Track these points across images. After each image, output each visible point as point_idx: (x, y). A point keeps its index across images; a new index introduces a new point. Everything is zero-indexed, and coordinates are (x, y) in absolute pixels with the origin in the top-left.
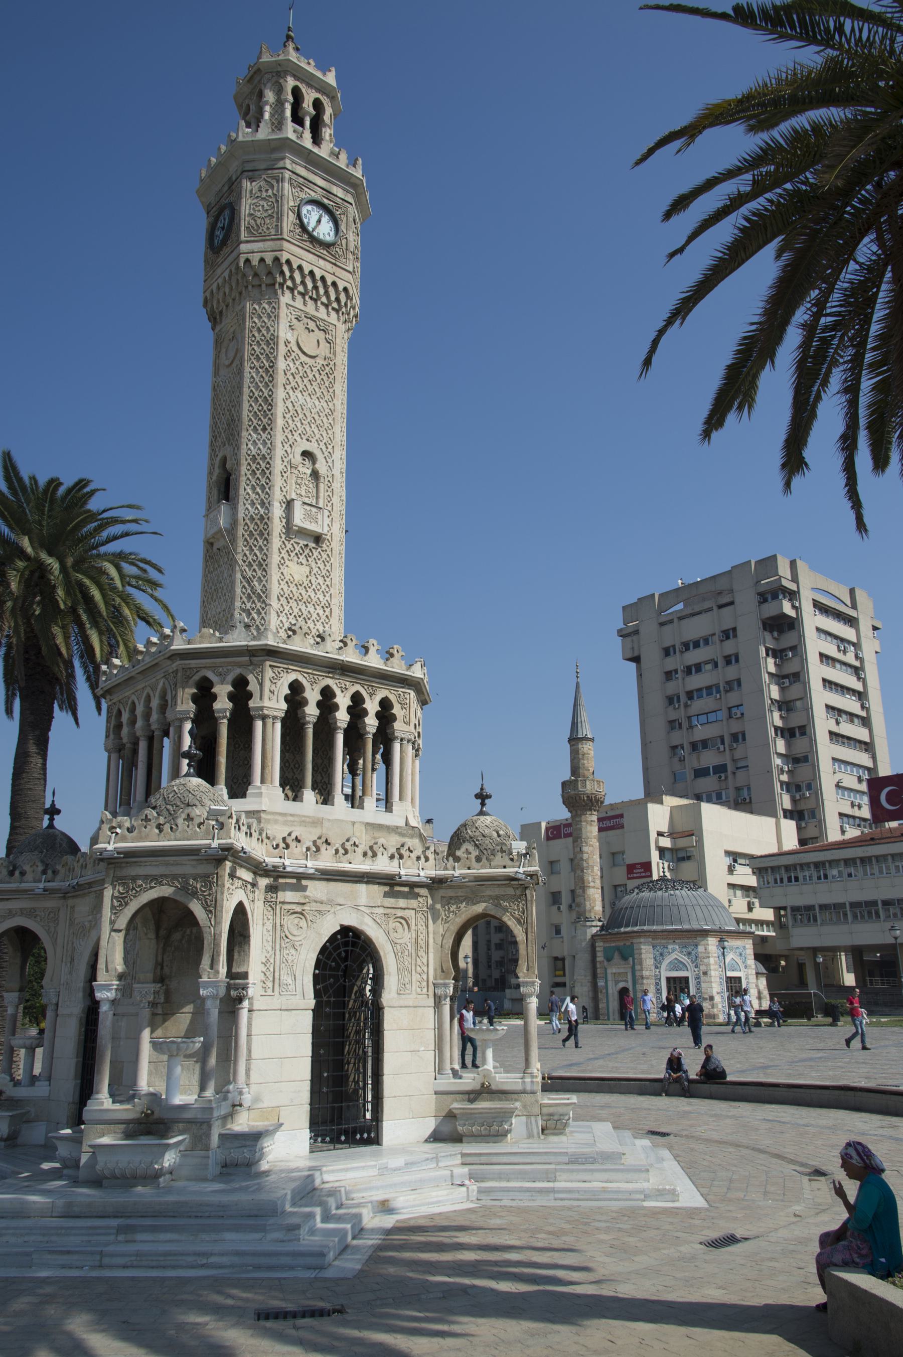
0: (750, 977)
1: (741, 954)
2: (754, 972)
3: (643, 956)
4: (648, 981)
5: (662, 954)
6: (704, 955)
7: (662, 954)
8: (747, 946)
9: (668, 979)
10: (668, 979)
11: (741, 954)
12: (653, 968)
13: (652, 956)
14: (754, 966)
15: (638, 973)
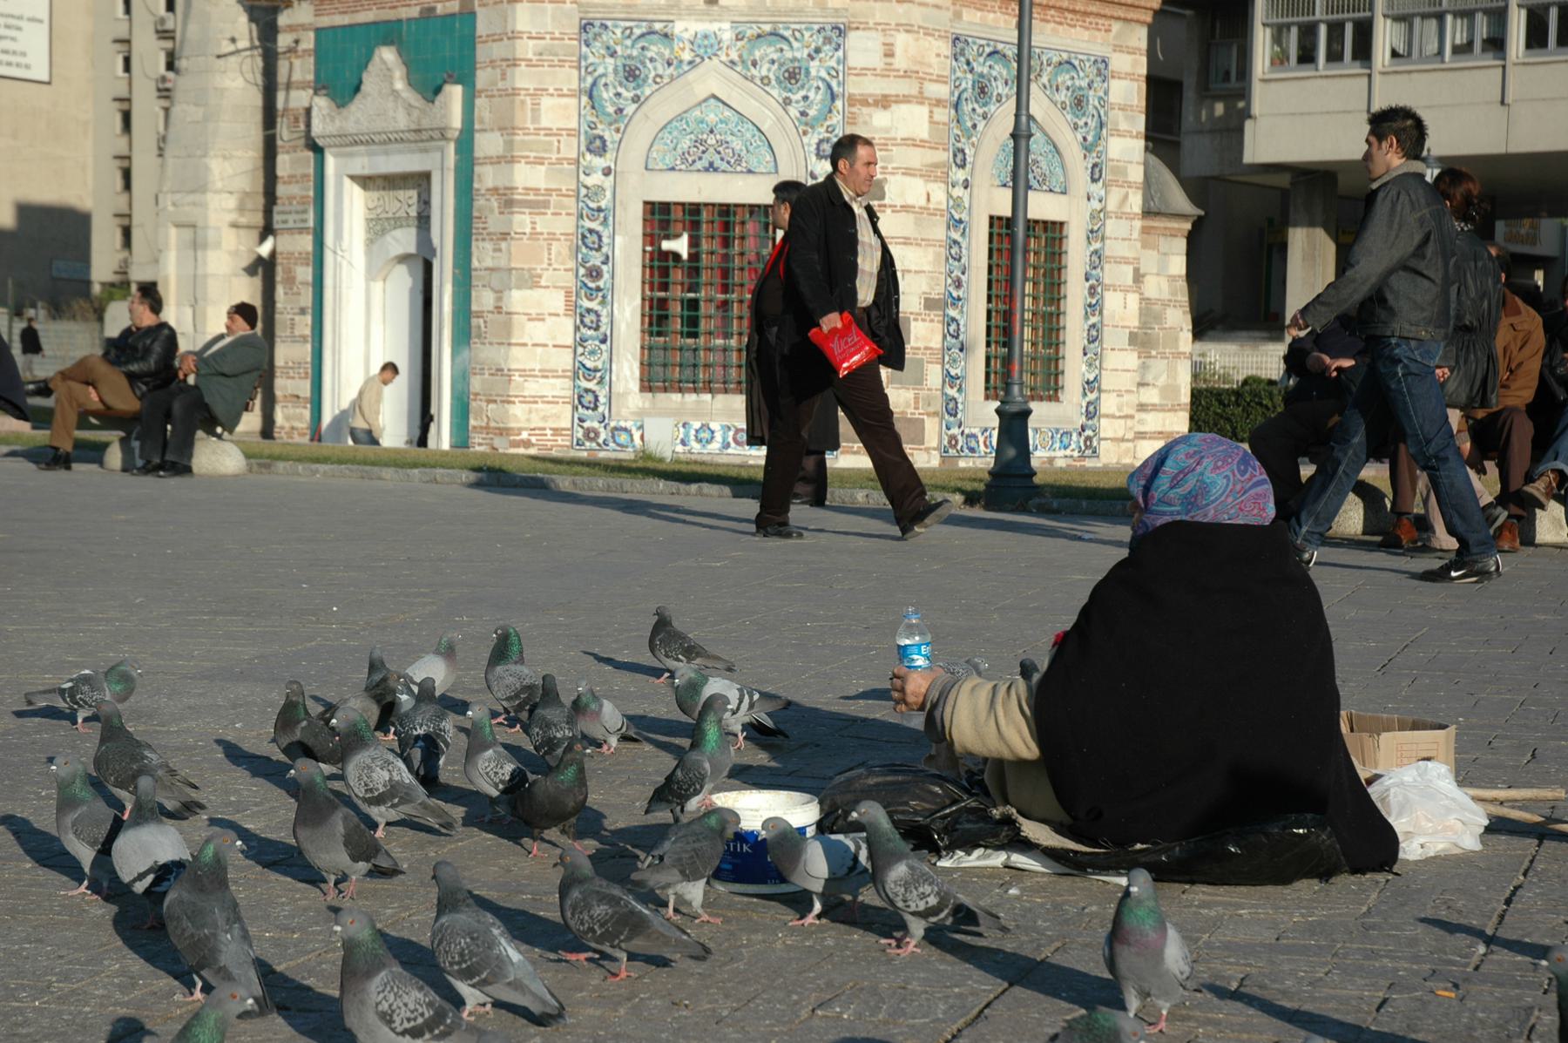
0: (1112, 227)
1: (1079, 103)
2: (1136, 202)
3: (523, 79)
4: (544, 224)
5: (631, 74)
6: (874, 87)
7: (631, 74)
8: (1120, 62)
9: (660, 217)
10: (660, 217)
11: (1079, 103)
12: (570, 148)
13: (569, 78)
14: (1136, 174)
15: (487, 177)
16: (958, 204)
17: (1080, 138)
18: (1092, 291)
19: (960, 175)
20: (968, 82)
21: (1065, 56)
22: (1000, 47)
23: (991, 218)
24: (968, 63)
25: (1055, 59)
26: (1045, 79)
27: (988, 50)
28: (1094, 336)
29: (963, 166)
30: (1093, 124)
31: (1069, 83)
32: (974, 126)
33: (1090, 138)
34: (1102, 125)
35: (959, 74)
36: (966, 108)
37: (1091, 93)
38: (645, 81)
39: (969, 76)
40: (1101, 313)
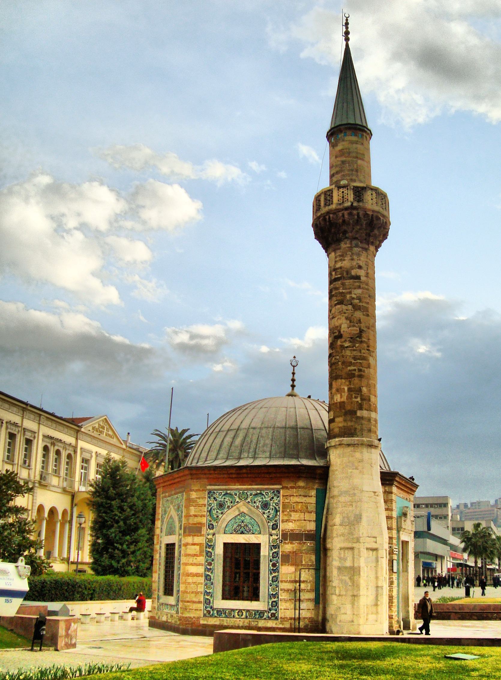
11: (265, 506)
16: (210, 540)
17: (265, 516)
18: (274, 565)
19: (211, 531)
20: (215, 504)
21: (259, 492)
22: (228, 492)
23: (225, 544)
24: (215, 498)
25: (254, 492)
26: (249, 500)
27: (223, 494)
28: (275, 579)
29: (213, 528)
30: (272, 512)
31: (261, 500)
32: (218, 517)
33: (271, 516)
34: (277, 511)
35: (210, 502)
36: (214, 512)
37: (272, 502)
38: (263, 509)
39: (215, 502)
40: (278, 572)
